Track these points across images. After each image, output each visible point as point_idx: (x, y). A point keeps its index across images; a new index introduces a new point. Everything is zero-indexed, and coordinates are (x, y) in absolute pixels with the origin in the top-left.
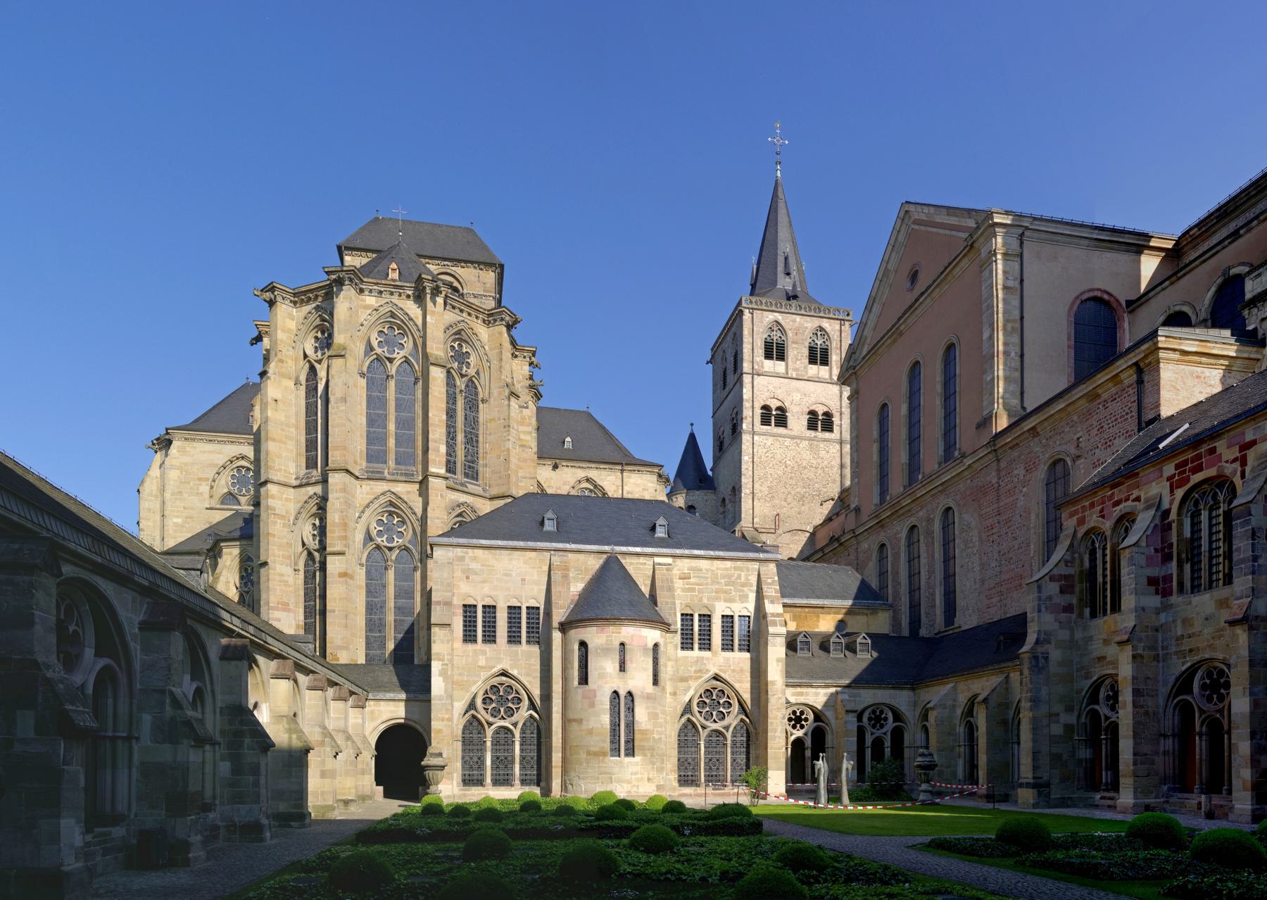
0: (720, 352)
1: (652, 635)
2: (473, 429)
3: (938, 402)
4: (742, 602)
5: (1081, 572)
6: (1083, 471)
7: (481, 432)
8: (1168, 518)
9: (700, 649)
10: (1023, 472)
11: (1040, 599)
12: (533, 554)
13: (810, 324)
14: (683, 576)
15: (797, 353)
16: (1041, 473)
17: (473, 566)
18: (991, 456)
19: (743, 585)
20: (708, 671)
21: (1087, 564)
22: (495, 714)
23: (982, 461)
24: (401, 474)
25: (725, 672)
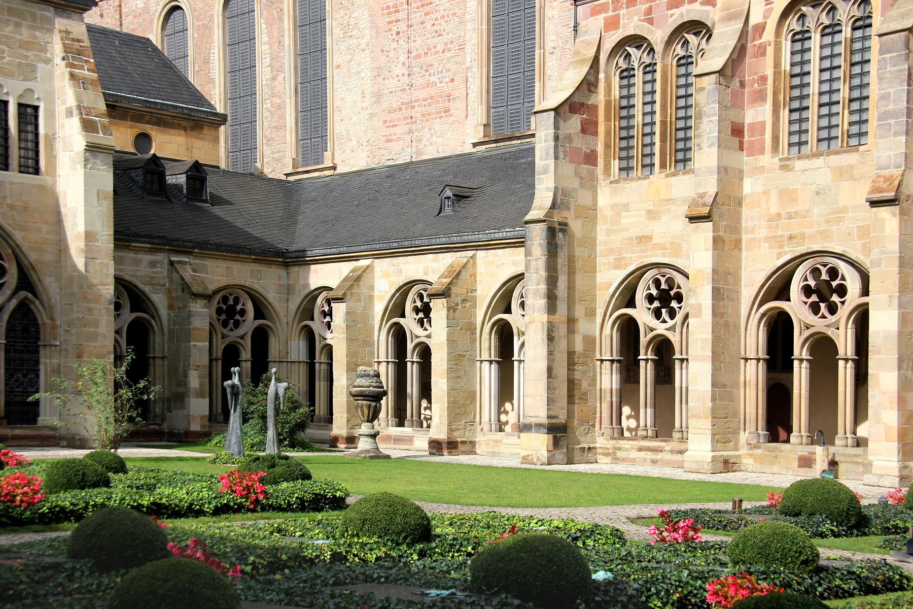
5: (608, 104)
8: (761, 37)
21: (616, 92)
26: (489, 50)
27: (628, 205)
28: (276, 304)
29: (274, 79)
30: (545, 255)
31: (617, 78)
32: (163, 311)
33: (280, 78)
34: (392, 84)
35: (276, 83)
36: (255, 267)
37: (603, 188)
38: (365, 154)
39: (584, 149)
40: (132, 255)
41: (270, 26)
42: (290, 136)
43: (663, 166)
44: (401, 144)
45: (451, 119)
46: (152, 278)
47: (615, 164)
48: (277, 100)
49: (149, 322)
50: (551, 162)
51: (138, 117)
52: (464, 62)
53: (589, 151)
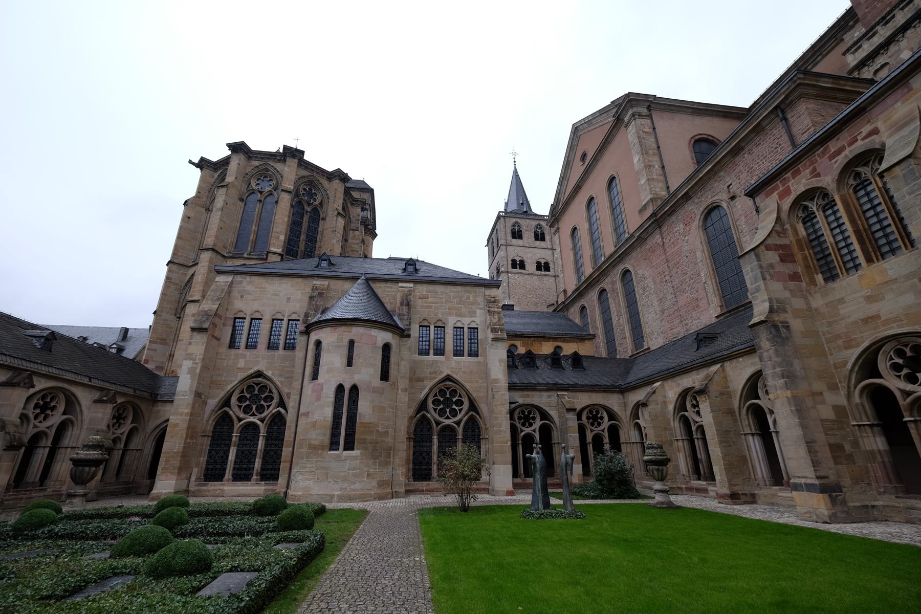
0: (491, 240)
1: (384, 337)
2: (314, 234)
3: (608, 212)
4: (471, 317)
5: (799, 241)
6: (739, 207)
7: (318, 236)
9: (435, 354)
10: (682, 226)
11: (761, 267)
12: (300, 280)
13: (535, 223)
14: (422, 296)
15: (528, 236)
16: (696, 223)
17: (249, 288)
18: (654, 225)
19: (472, 304)
20: (441, 372)
22: (248, 411)
23: (647, 231)
24: (255, 255)
25: (457, 374)
26: (713, 271)
27: (843, 298)
28: (619, 413)
29: (619, 320)
30: (774, 346)
31: (801, 224)
32: (556, 419)
33: (621, 318)
34: (668, 303)
35: (620, 321)
36: (605, 394)
37: (814, 295)
38: (661, 339)
39: (787, 272)
40: (538, 393)
41: (614, 300)
42: (629, 340)
43: (869, 260)
44: (678, 329)
45: (701, 310)
46: (549, 403)
47: (819, 278)
48: (621, 328)
49: (550, 425)
50: (761, 283)
51: (555, 339)
52: (702, 281)
53: (792, 273)
